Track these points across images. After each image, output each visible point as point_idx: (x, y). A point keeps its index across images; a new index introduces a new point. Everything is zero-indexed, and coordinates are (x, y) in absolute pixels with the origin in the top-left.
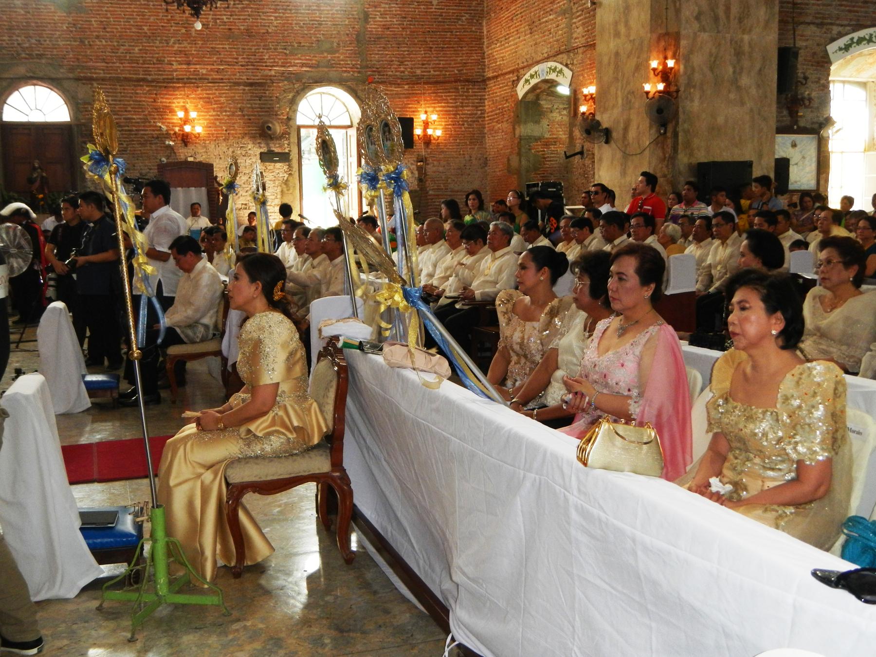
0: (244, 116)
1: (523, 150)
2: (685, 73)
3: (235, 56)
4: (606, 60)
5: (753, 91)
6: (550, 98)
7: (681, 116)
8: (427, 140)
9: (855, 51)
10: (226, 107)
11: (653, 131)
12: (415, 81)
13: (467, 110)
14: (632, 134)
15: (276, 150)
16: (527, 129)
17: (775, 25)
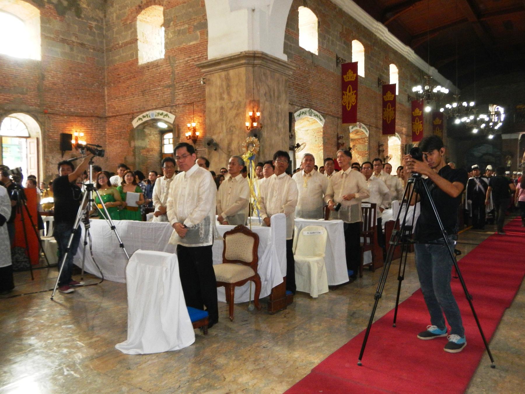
1: (136, 154)
4: (213, 110)
5: (282, 130)
6: (150, 128)
9: (301, 116)
13: (97, 132)
14: (234, 146)
16: (138, 143)
17: (288, 102)
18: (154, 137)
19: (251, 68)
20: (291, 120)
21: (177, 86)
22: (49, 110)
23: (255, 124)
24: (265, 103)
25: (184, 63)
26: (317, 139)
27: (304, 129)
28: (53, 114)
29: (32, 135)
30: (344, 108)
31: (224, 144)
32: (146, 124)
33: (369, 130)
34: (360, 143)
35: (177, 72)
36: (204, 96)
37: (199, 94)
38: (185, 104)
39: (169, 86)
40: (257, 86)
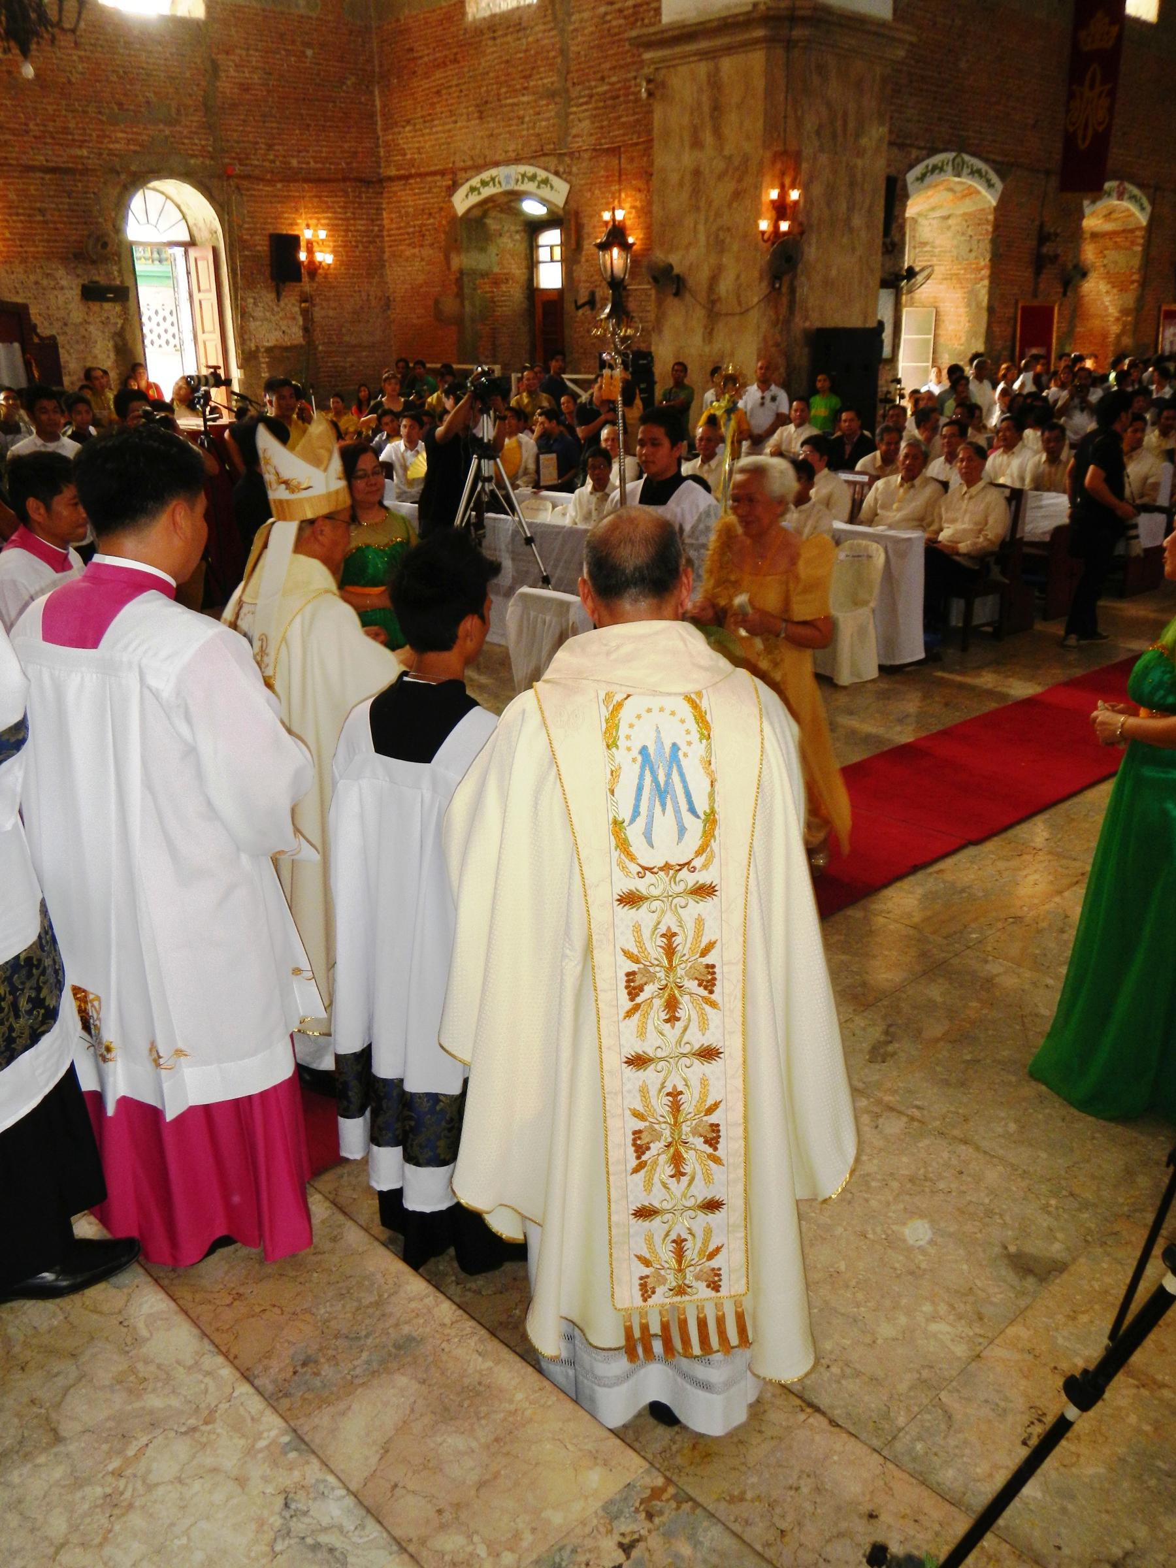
0: (45, 222)
1: (466, 291)
2: (805, 207)
3: (23, 120)
4: (674, 178)
5: (863, 234)
7: (800, 266)
8: (314, 269)
9: (928, 180)
10: (17, 207)
11: (764, 284)
12: (291, 177)
13: (361, 225)
14: (725, 286)
15: (102, 280)
18: (511, 241)
19: (780, 52)
20: (895, 195)
21: (574, 92)
22: (238, 169)
23: (784, 226)
24: (815, 159)
25: (596, 20)
26: (975, 247)
27: (938, 213)
28: (248, 177)
29: (198, 239)
30: (1069, 140)
31: (699, 279)
32: (490, 205)
33: (1153, 203)
34: (1117, 247)
35: (574, 49)
36: (649, 132)
37: (638, 121)
38: (598, 152)
39: (552, 95)
40: (796, 111)
